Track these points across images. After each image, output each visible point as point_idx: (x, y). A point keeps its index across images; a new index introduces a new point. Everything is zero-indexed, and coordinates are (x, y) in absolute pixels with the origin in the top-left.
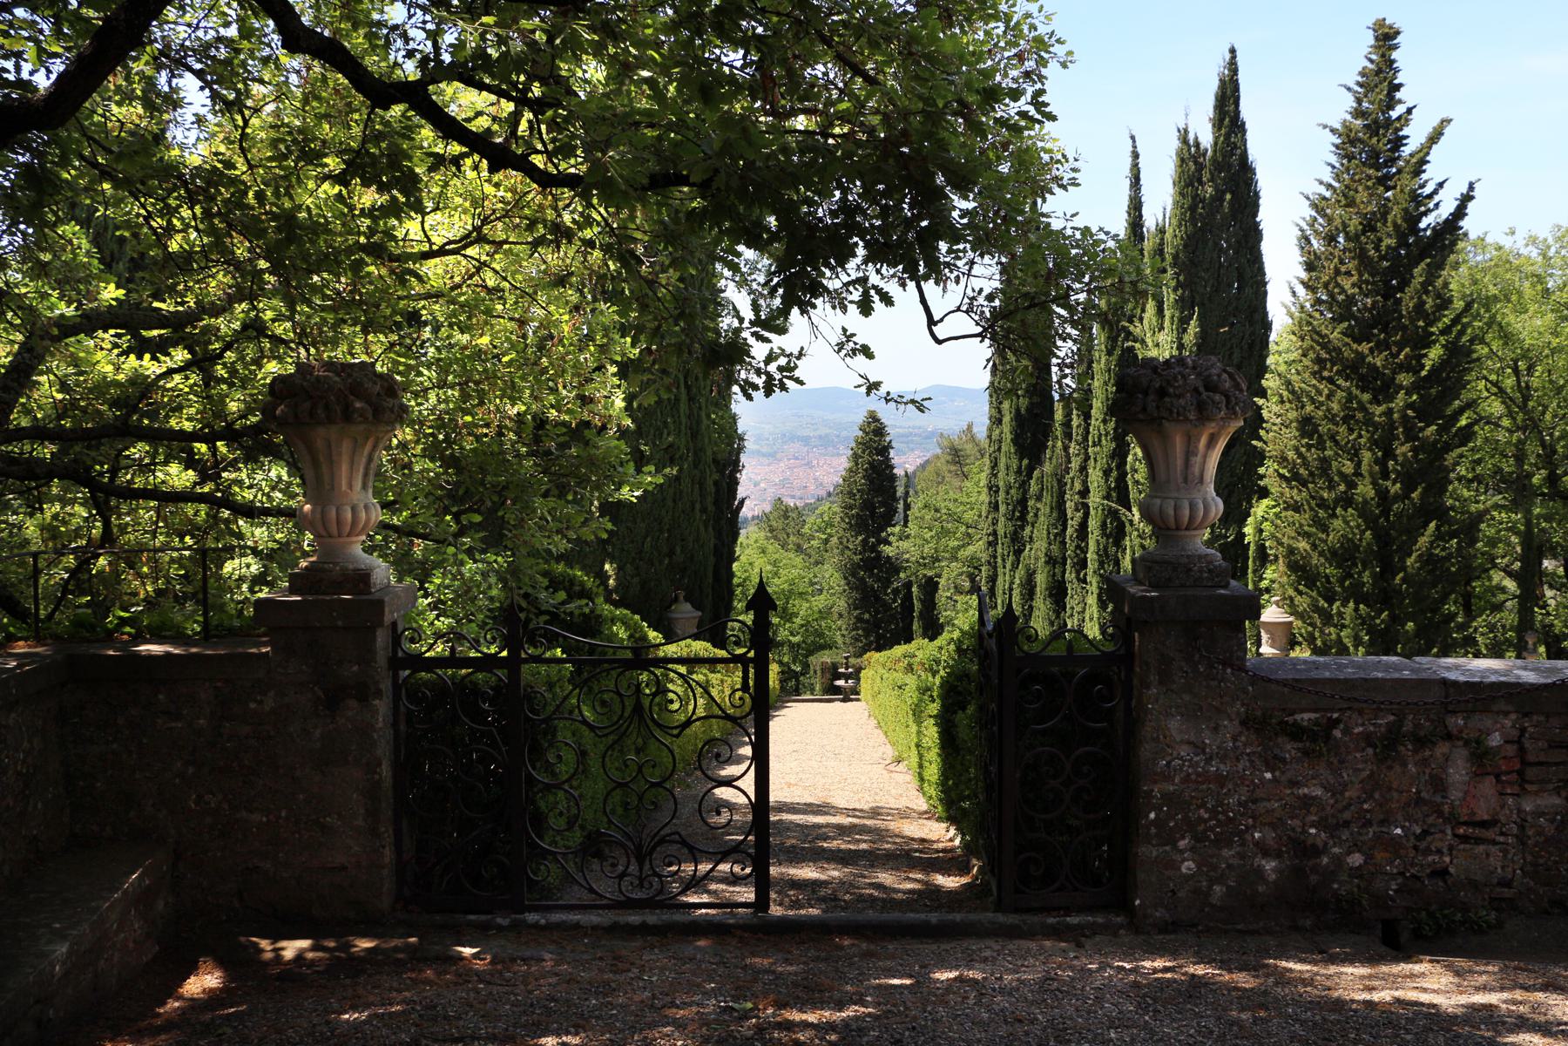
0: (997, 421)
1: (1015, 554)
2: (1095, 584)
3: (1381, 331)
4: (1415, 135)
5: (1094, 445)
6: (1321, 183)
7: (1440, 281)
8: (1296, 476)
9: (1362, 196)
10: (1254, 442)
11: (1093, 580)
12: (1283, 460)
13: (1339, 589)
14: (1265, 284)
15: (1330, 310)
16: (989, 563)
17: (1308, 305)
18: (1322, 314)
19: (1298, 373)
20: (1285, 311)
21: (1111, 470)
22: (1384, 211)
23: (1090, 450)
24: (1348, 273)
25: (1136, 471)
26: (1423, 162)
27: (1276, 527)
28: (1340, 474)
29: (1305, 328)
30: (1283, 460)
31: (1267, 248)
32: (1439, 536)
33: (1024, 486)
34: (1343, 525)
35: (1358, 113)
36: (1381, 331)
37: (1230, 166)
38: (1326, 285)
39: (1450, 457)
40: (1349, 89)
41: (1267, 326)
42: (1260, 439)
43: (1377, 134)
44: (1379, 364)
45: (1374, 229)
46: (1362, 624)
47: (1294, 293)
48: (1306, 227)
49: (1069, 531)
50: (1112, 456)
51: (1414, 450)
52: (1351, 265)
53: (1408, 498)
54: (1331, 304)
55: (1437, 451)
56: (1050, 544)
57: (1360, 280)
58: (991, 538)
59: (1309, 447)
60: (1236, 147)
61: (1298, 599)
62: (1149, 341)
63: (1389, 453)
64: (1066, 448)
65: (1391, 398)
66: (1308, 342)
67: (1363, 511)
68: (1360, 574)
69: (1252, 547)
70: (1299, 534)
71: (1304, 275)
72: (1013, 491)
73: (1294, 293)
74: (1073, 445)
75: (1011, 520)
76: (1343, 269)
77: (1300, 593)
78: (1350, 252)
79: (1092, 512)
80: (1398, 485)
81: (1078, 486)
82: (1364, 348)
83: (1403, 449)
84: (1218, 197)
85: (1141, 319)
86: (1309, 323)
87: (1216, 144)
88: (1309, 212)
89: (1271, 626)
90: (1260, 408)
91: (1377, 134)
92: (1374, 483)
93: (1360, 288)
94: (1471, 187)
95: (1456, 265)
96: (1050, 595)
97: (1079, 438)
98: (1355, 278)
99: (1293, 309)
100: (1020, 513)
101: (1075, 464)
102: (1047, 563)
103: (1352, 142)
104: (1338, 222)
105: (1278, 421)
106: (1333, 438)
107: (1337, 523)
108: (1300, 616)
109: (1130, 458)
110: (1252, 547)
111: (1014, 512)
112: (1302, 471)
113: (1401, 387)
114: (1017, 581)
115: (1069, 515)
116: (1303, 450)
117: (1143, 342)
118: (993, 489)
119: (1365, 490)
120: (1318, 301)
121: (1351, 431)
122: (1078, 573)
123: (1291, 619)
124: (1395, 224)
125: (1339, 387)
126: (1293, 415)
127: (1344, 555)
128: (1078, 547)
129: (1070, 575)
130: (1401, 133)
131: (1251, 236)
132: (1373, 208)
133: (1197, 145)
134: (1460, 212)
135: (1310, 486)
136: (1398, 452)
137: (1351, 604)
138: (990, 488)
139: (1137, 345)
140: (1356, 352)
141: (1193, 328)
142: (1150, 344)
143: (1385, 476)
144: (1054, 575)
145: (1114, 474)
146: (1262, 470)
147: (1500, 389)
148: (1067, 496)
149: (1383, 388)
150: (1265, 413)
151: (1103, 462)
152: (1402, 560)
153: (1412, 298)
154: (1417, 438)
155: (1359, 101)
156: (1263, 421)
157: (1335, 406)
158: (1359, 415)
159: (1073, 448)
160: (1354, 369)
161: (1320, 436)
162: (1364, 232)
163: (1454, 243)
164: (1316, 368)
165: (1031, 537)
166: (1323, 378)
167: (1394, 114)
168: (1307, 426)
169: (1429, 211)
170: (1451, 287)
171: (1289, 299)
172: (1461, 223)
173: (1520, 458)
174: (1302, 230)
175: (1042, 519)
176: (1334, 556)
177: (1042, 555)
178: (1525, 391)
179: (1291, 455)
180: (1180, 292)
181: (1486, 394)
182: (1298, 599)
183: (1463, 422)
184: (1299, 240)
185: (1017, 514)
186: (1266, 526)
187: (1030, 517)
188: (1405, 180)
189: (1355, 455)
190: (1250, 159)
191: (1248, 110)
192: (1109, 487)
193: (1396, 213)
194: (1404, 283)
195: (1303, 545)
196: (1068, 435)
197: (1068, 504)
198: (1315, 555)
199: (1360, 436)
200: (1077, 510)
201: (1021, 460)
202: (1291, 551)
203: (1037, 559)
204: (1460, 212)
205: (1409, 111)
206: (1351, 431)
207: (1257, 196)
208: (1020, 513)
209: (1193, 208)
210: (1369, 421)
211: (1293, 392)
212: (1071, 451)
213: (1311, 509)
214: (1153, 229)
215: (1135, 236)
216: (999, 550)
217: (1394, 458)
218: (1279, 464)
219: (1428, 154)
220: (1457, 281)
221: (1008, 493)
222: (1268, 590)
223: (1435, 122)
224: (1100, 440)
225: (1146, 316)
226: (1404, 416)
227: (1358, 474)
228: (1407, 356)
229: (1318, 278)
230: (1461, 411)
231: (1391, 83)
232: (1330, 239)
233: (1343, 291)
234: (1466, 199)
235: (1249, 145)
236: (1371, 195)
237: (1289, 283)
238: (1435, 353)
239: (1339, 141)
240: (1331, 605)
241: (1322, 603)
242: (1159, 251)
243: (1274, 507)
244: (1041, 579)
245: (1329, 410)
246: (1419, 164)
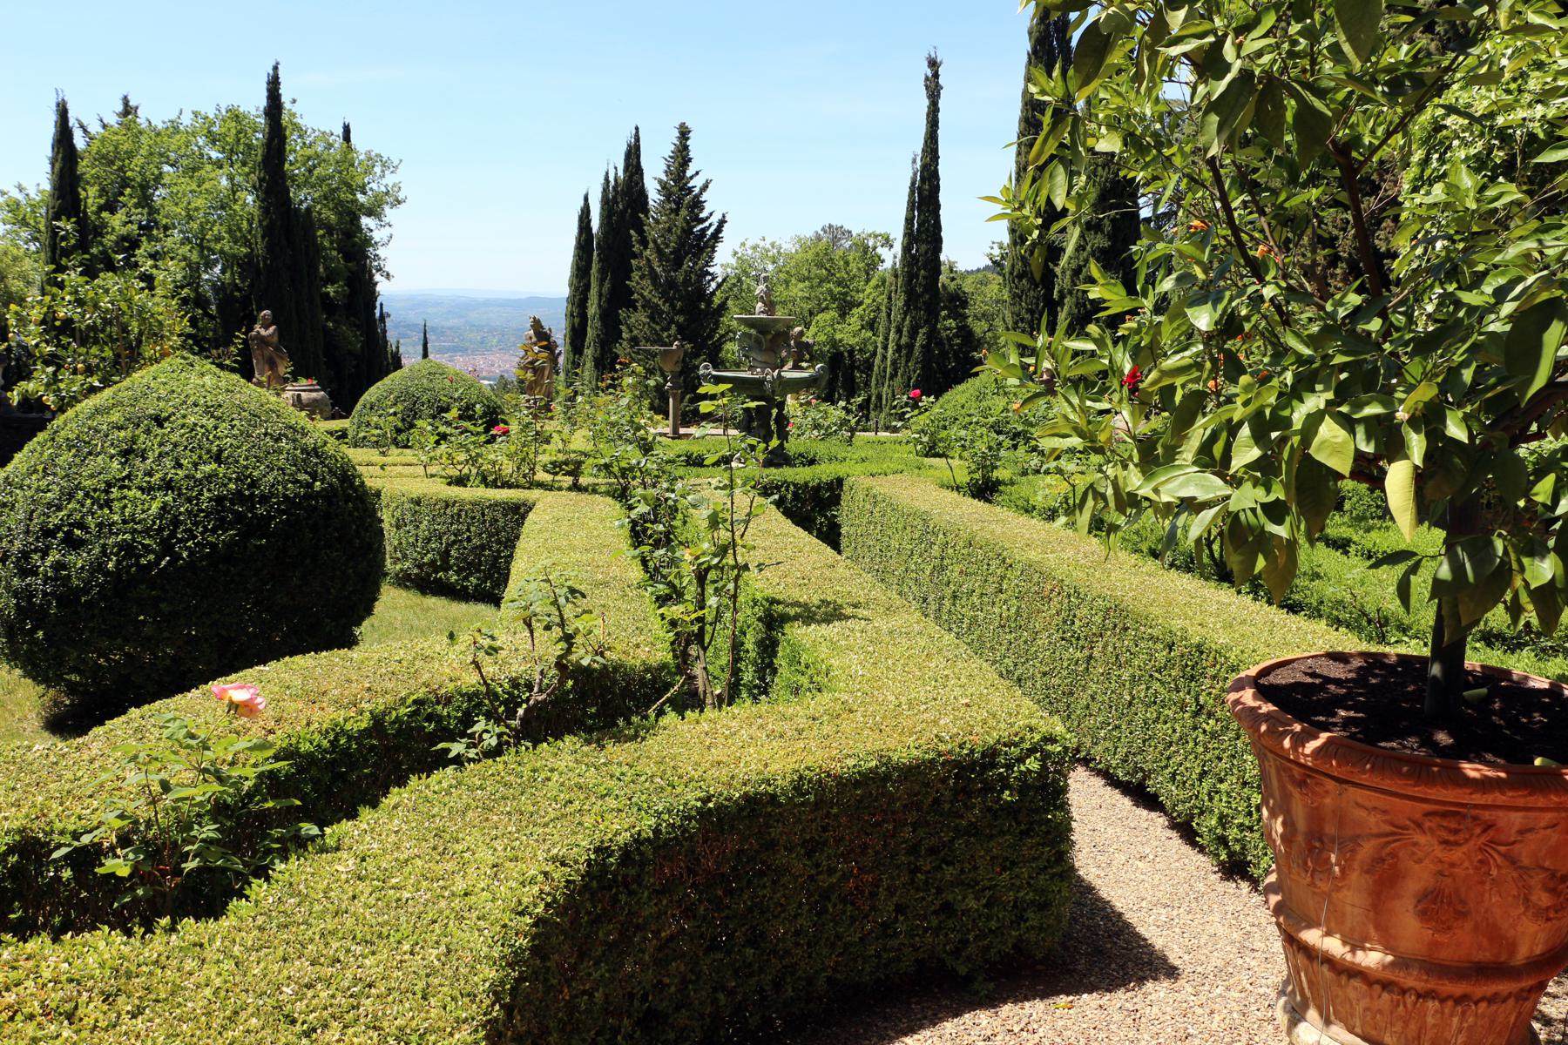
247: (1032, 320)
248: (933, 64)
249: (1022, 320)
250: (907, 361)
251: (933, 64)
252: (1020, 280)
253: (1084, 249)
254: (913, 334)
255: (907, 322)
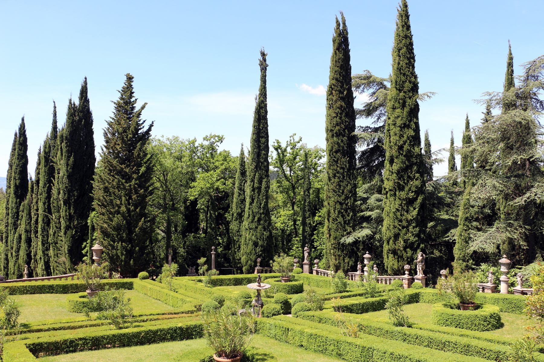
0: (9, 187)
1: (15, 228)
2: (41, 238)
3: (128, 162)
4: (138, 107)
5: (40, 195)
6: (111, 118)
7: (144, 148)
8: (103, 205)
9: (123, 122)
10: (90, 194)
11: (40, 237)
12: (99, 200)
13: (116, 238)
14: (94, 147)
15: (113, 155)
16: (6, 232)
17: (106, 153)
18: (111, 156)
19: (104, 174)
20: (99, 155)
21: (46, 203)
22: (129, 127)
23: (39, 196)
24: (119, 145)
25: (54, 203)
26: (140, 114)
27: (97, 220)
28: (116, 204)
29: (105, 160)
30: (99, 200)
31: (95, 136)
32: (145, 222)
33: (18, 208)
34: (117, 219)
35: (122, 98)
36: (128, 162)
37: (84, 112)
38: (112, 148)
39: (148, 199)
40: (119, 92)
41: (95, 160)
42: (92, 193)
43: (127, 105)
44: (127, 171)
45: (126, 132)
46: (124, 249)
47: (102, 150)
48: (106, 130)
49: (32, 222)
50: (46, 198)
51: (137, 197)
52: (119, 142)
53: (136, 211)
54: (113, 153)
55: (144, 197)
56: (26, 226)
57: (122, 146)
58: (7, 224)
59: (107, 196)
60: (86, 106)
61: (104, 242)
62: (58, 163)
63: (130, 198)
64: (32, 196)
65: (131, 181)
66: (106, 164)
67: (123, 215)
68: (122, 234)
69: (90, 226)
70: (104, 222)
71: (105, 144)
72: (14, 209)
73: (102, 150)
74: (34, 195)
75: (13, 218)
76: (117, 143)
77: (105, 240)
78: (119, 138)
79: (40, 216)
80: (133, 207)
81: (35, 208)
82: (123, 166)
83: (134, 196)
84: (80, 120)
85: (56, 156)
86: (107, 159)
87: (80, 104)
88: (107, 126)
89: (96, 251)
90: (92, 184)
91: (127, 105)
92: (126, 207)
93: (122, 149)
94: (153, 123)
95: (149, 144)
96: (26, 242)
97: (36, 193)
98: (120, 146)
99: (102, 154)
100: (17, 216)
101: (34, 201)
102: (25, 232)
103: (120, 107)
104: (115, 129)
105: (98, 188)
106: (114, 193)
107: (115, 219)
108: (105, 247)
109: (52, 199)
110: (90, 226)
111: (14, 216)
112: (105, 203)
113: (133, 178)
114: (15, 238)
115: (32, 217)
116: (105, 197)
117: (56, 163)
118: (7, 208)
119: (123, 209)
120: (110, 152)
121: (119, 191)
122: (35, 235)
123: (102, 248)
124: (132, 131)
125: (116, 178)
126: (102, 186)
127: (118, 228)
128: (35, 227)
129: (33, 236)
130: (134, 106)
131: (91, 133)
132: (125, 126)
133: (74, 105)
134: (149, 130)
135: (107, 207)
136: (133, 197)
137: (120, 243)
138: (6, 208)
139: (54, 164)
140: (121, 167)
141: (72, 159)
142: (59, 164)
143: (129, 204)
144: (28, 235)
145: (47, 204)
146: (93, 203)
147: (159, 180)
148: (32, 211)
149: (128, 178)
150: (94, 186)
151: (43, 200)
152: (135, 229)
153: (137, 152)
154: (138, 193)
155: (122, 95)
156: (93, 188)
157: (115, 183)
158: (122, 186)
159: (34, 196)
160: (120, 173)
161: (110, 193)
162: (123, 133)
163: (148, 138)
164: (109, 172)
165: (20, 224)
166: (111, 175)
167: (132, 100)
168: (106, 190)
169: (141, 128)
170: (148, 150)
171: (101, 151)
172: (150, 133)
173: (164, 199)
174: (105, 131)
175: (24, 218)
176: (114, 229)
177: (23, 229)
178: (166, 180)
179: (101, 198)
180: (68, 148)
181: (156, 181)
182: (104, 242)
183: (150, 189)
184: (104, 134)
185: (15, 216)
186: (94, 221)
187: (20, 217)
188: (135, 118)
189: (120, 198)
190: (90, 110)
191: (90, 96)
192: (45, 208)
193: (132, 128)
194: (134, 148)
195: (105, 225)
196: (32, 191)
197: (32, 213)
198: (109, 228)
199: (122, 193)
200: (35, 215)
201: (17, 199)
202: (102, 227)
203: (22, 230)
204: (149, 130)
205: (136, 100)
206: (119, 191)
207: (92, 121)
208: (17, 216)
209: (72, 123)
210: (124, 188)
211: (102, 179)
212: (33, 196)
213: (108, 215)
214: (61, 129)
215: (54, 131)
216: (9, 228)
217: (132, 199)
218: (98, 201)
219: (141, 112)
220: (149, 148)
221: (12, 210)
222: (95, 239)
223: (143, 104)
224: (42, 193)
225: (58, 155)
226: (135, 187)
227: (121, 204)
228: (135, 169)
229: (110, 145)
230: (149, 186)
231: (131, 91)
232: (113, 134)
233: (117, 149)
234: (151, 126)
235: (90, 106)
236: (125, 122)
237: (101, 147)
238: (143, 169)
239: (116, 106)
240: (114, 243)
241: (112, 243)
242: (62, 136)
243: (97, 214)
244: (23, 237)
245: (113, 185)
246: (139, 114)
247: (343, 173)
248: (263, 55)
249: (338, 172)
250: (259, 195)
251: (263, 55)
252: (336, 154)
253: (403, 137)
254: (260, 182)
255: (257, 176)
